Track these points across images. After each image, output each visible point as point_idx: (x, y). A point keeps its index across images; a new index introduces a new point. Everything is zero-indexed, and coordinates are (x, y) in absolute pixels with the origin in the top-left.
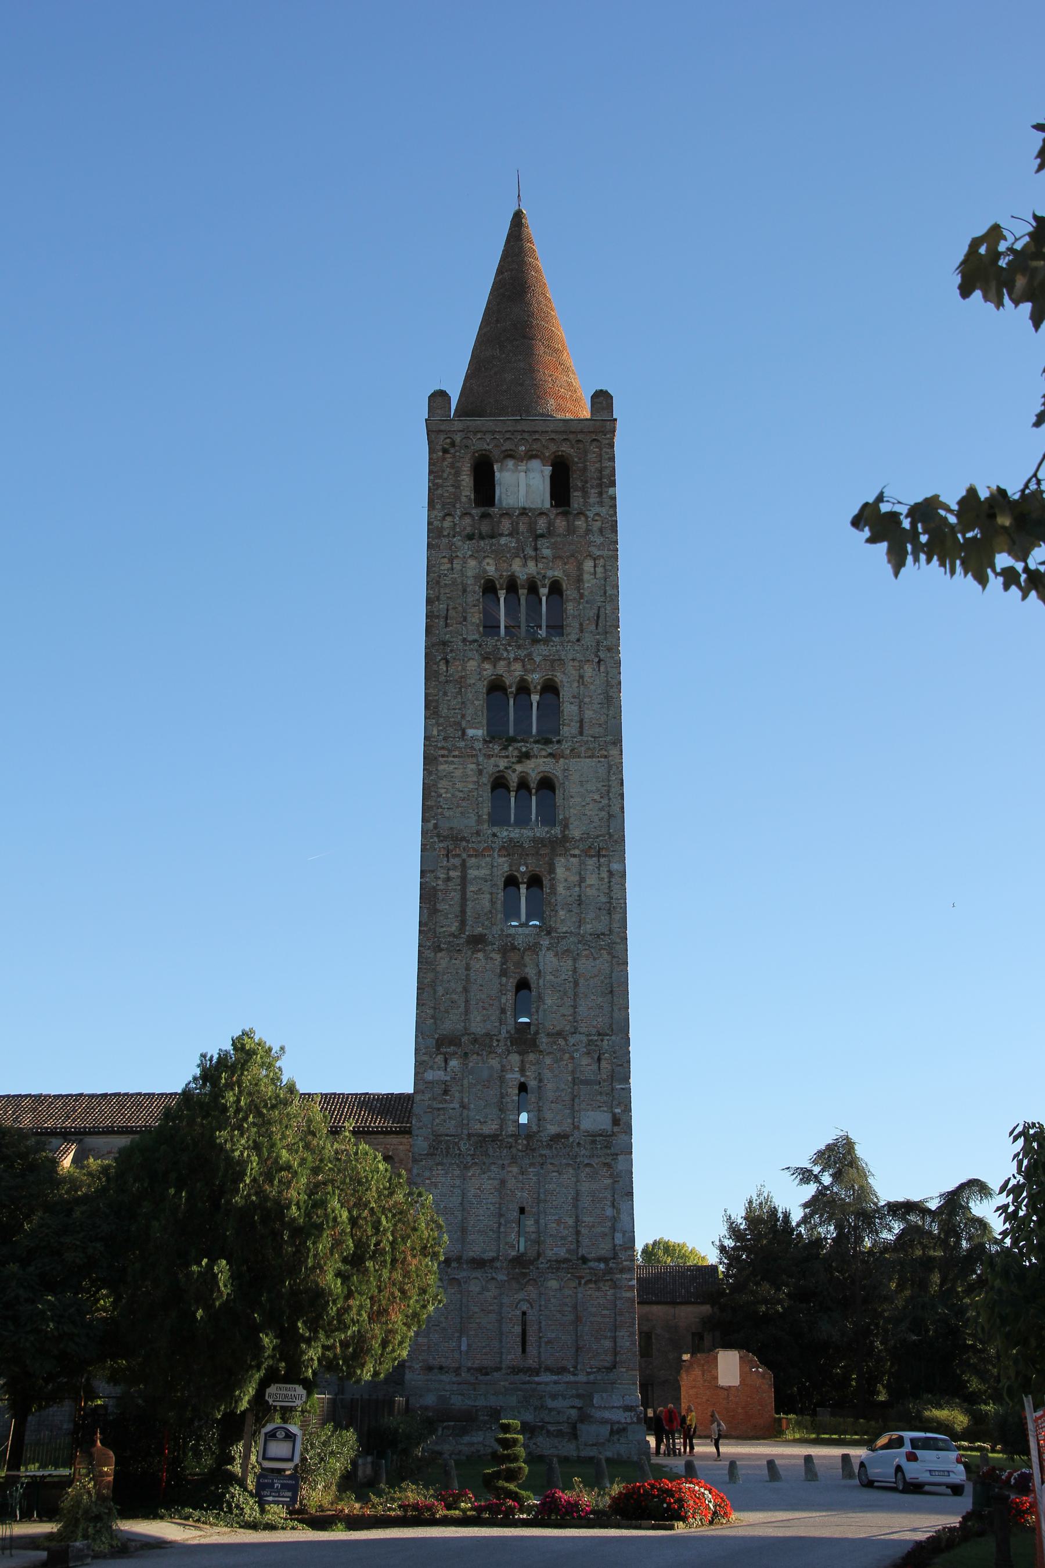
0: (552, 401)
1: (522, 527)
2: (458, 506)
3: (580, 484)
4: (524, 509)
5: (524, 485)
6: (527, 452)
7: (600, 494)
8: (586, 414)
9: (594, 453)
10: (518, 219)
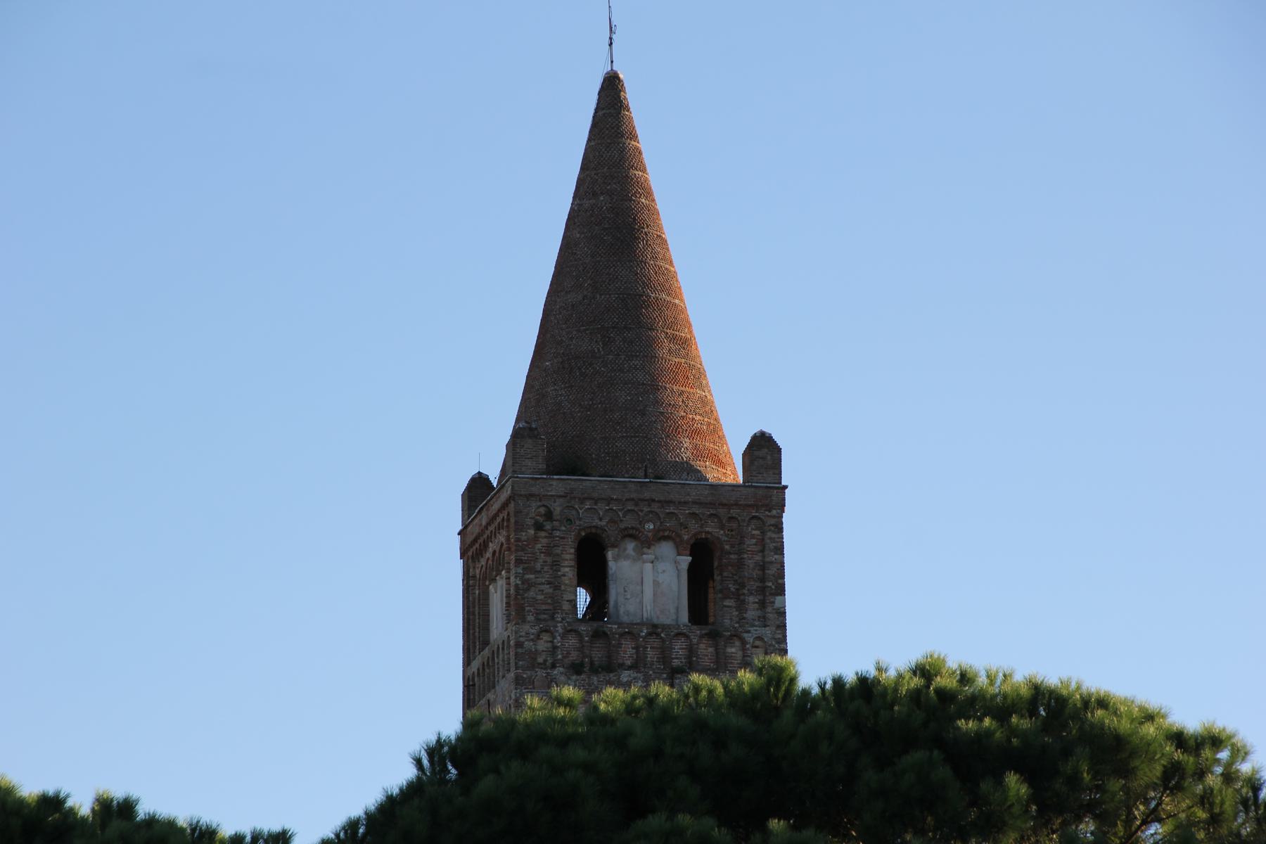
0: (686, 443)
1: (651, 655)
2: (559, 617)
3: (732, 588)
4: (655, 626)
5: (651, 582)
6: (656, 531)
7: (763, 605)
8: (741, 480)
9: (753, 537)
10: (611, 88)
